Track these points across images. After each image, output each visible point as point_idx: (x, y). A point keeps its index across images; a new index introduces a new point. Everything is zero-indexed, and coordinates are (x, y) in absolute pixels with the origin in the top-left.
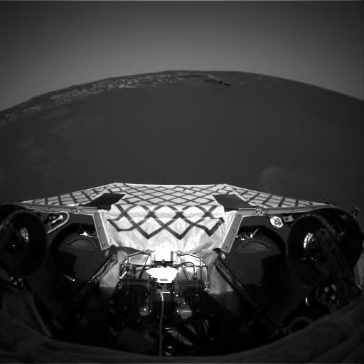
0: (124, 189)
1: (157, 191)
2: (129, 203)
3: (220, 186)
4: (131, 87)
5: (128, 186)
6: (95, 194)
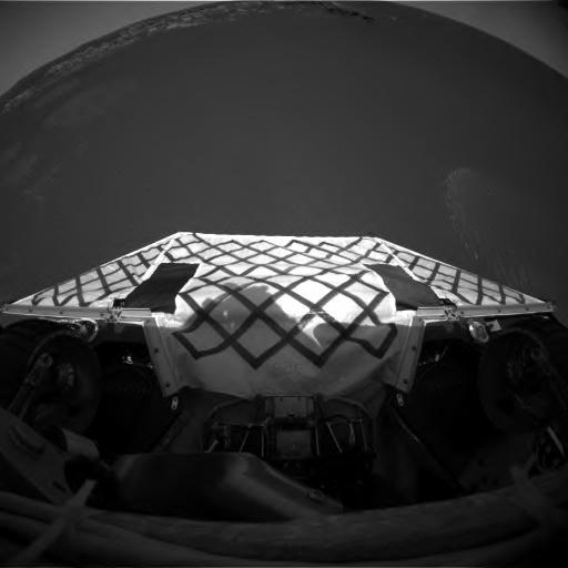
0: (195, 248)
1: (259, 252)
2: (206, 281)
3: (368, 243)
4: (189, 25)
5: (201, 241)
6: (143, 267)
